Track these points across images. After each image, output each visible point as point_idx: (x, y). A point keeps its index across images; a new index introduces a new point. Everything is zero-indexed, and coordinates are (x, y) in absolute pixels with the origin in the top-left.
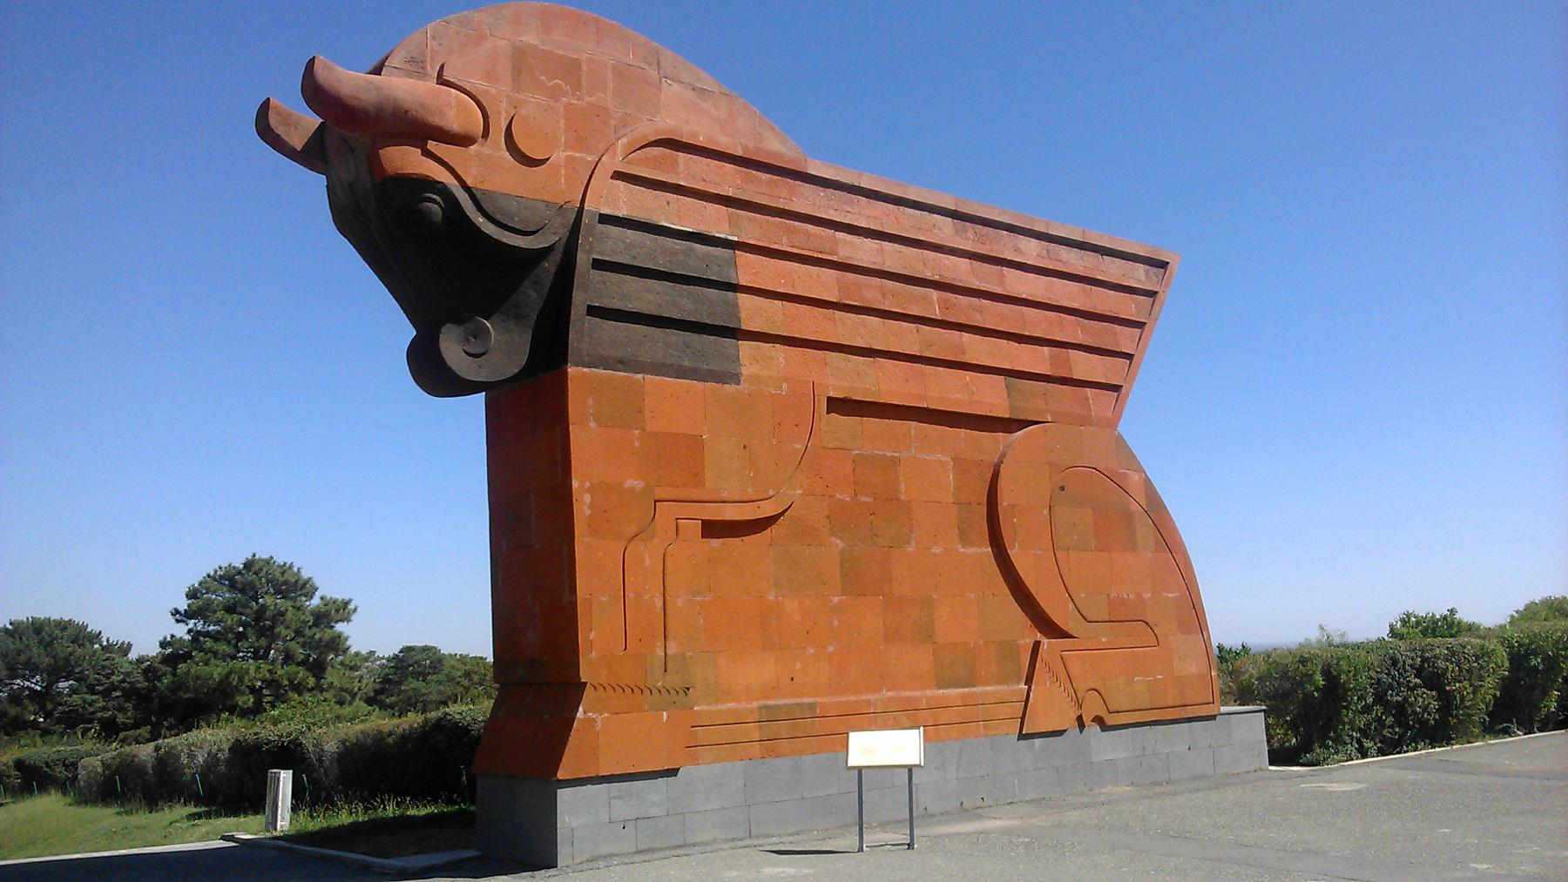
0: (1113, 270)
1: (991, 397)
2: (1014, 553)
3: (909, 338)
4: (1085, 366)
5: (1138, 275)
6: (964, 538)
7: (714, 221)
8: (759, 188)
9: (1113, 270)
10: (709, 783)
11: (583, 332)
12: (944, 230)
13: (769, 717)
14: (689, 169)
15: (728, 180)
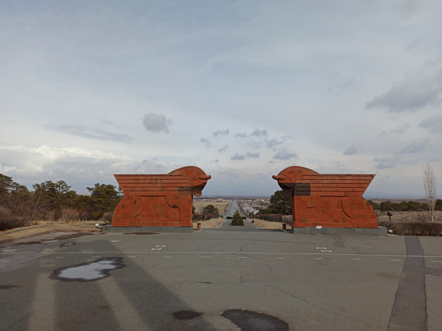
0: (362, 178)
1: (343, 194)
2: (344, 210)
3: (331, 189)
4: (356, 189)
5: (368, 178)
6: (338, 208)
7: (308, 182)
8: (313, 178)
9: (362, 178)
10: (308, 229)
11: (295, 193)
12: (336, 178)
13: (313, 224)
14: (305, 178)
15: (310, 178)
